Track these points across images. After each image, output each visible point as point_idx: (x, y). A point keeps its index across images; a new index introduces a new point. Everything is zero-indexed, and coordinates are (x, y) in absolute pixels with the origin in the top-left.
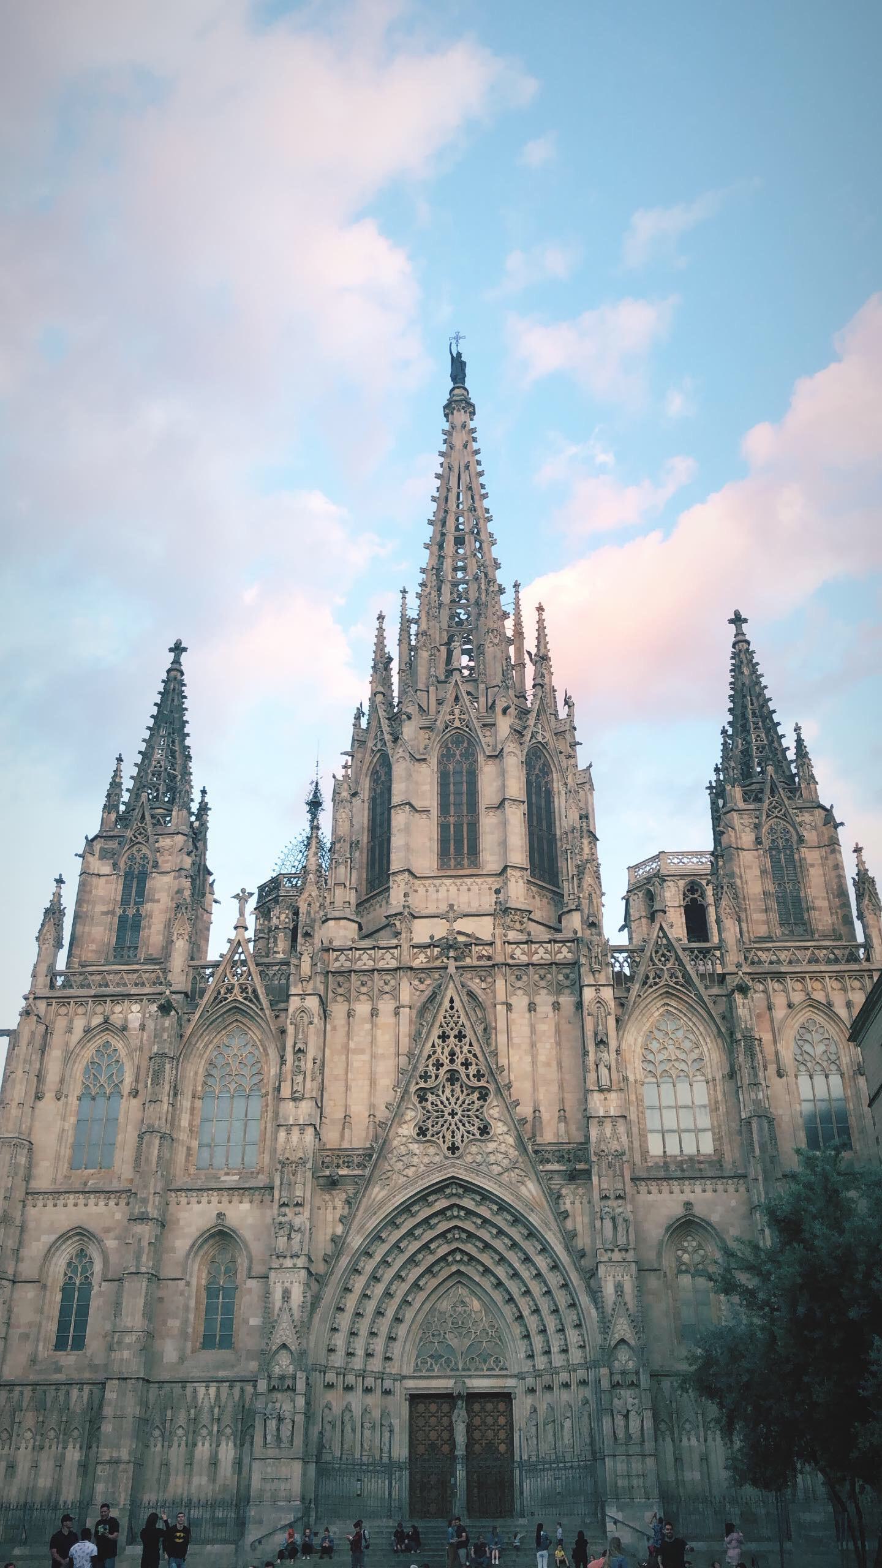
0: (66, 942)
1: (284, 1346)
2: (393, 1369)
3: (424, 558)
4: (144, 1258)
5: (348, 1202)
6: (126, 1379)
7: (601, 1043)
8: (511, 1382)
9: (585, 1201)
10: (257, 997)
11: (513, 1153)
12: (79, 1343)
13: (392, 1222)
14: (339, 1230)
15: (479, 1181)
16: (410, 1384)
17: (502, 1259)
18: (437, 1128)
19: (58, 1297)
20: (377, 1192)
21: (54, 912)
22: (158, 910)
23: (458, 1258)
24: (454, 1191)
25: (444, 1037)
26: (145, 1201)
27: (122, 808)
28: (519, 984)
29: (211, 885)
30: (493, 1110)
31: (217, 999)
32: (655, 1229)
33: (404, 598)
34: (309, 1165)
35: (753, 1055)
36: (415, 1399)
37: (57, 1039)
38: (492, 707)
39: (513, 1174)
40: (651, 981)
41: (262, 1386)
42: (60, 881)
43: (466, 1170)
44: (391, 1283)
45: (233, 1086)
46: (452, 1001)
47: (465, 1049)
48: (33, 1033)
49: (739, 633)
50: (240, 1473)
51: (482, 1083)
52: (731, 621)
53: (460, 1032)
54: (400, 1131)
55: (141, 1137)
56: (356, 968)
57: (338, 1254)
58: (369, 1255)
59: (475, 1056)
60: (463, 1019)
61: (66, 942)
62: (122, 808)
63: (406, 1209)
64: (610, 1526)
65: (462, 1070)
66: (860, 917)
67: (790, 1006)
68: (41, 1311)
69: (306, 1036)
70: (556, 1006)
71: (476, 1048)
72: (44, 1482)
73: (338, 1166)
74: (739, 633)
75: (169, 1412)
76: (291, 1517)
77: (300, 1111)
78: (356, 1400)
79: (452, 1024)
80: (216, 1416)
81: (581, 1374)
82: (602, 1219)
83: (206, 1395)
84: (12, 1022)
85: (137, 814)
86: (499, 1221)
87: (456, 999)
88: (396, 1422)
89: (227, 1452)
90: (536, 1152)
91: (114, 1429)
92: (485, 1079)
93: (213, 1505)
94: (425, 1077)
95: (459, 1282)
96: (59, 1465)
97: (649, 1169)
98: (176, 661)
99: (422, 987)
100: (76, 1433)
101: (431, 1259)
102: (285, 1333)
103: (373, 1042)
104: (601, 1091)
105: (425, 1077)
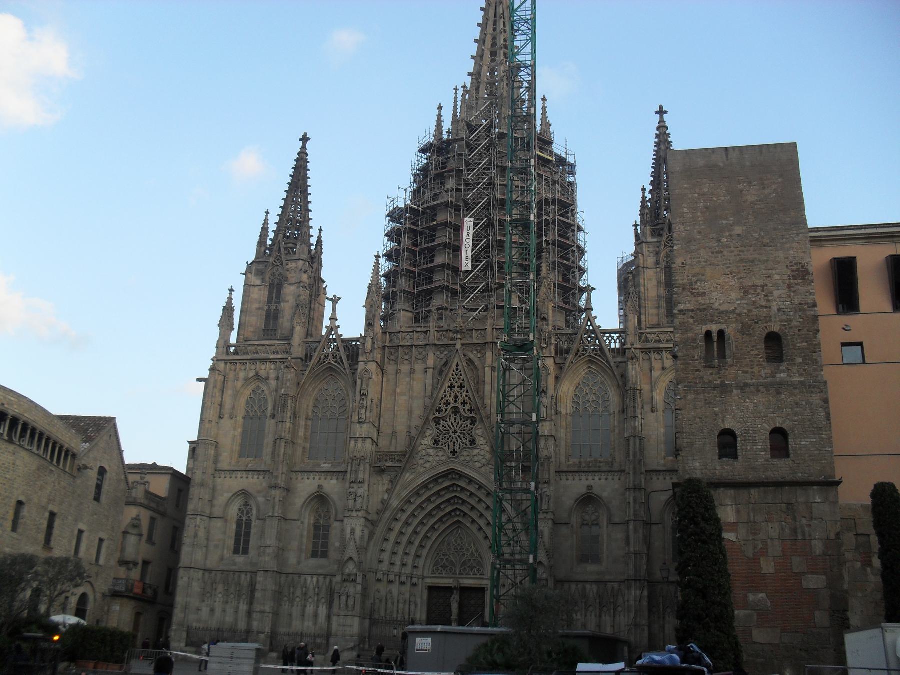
0: (236, 326)
1: (351, 559)
2: (419, 572)
3: (470, 66)
4: (277, 508)
5: (391, 482)
10: (342, 361)
11: (489, 456)
12: (246, 551)
13: (418, 494)
15: (467, 471)
16: (429, 581)
17: (482, 515)
19: (234, 526)
20: (408, 477)
21: (228, 310)
22: (287, 307)
25: (451, 387)
26: (277, 477)
27: (269, 243)
29: (325, 289)
30: (478, 432)
31: (320, 362)
32: (569, 501)
33: (456, 94)
34: (367, 461)
35: (635, 400)
36: (432, 589)
37: (230, 384)
41: (338, 579)
42: (231, 290)
44: (417, 526)
45: (328, 414)
46: (457, 365)
47: (464, 395)
48: (216, 381)
49: (662, 121)
52: (657, 113)
54: (423, 442)
55: (275, 442)
56: (401, 344)
57: (384, 510)
58: (403, 511)
59: (470, 398)
60: (464, 376)
61: (236, 326)
62: (269, 243)
63: (425, 486)
65: (461, 407)
67: (663, 369)
68: (225, 533)
69: (368, 386)
71: (470, 394)
72: (229, 619)
73: (386, 461)
74: (662, 121)
75: (292, 589)
76: (352, 645)
78: (395, 589)
83: (311, 582)
84: (206, 375)
85: (275, 248)
86: (479, 494)
88: (419, 601)
89: (323, 611)
93: (315, 637)
94: (439, 411)
96: (237, 612)
97: (569, 466)
98: (304, 148)
99: (442, 356)
100: (244, 597)
101: (442, 514)
102: (351, 552)
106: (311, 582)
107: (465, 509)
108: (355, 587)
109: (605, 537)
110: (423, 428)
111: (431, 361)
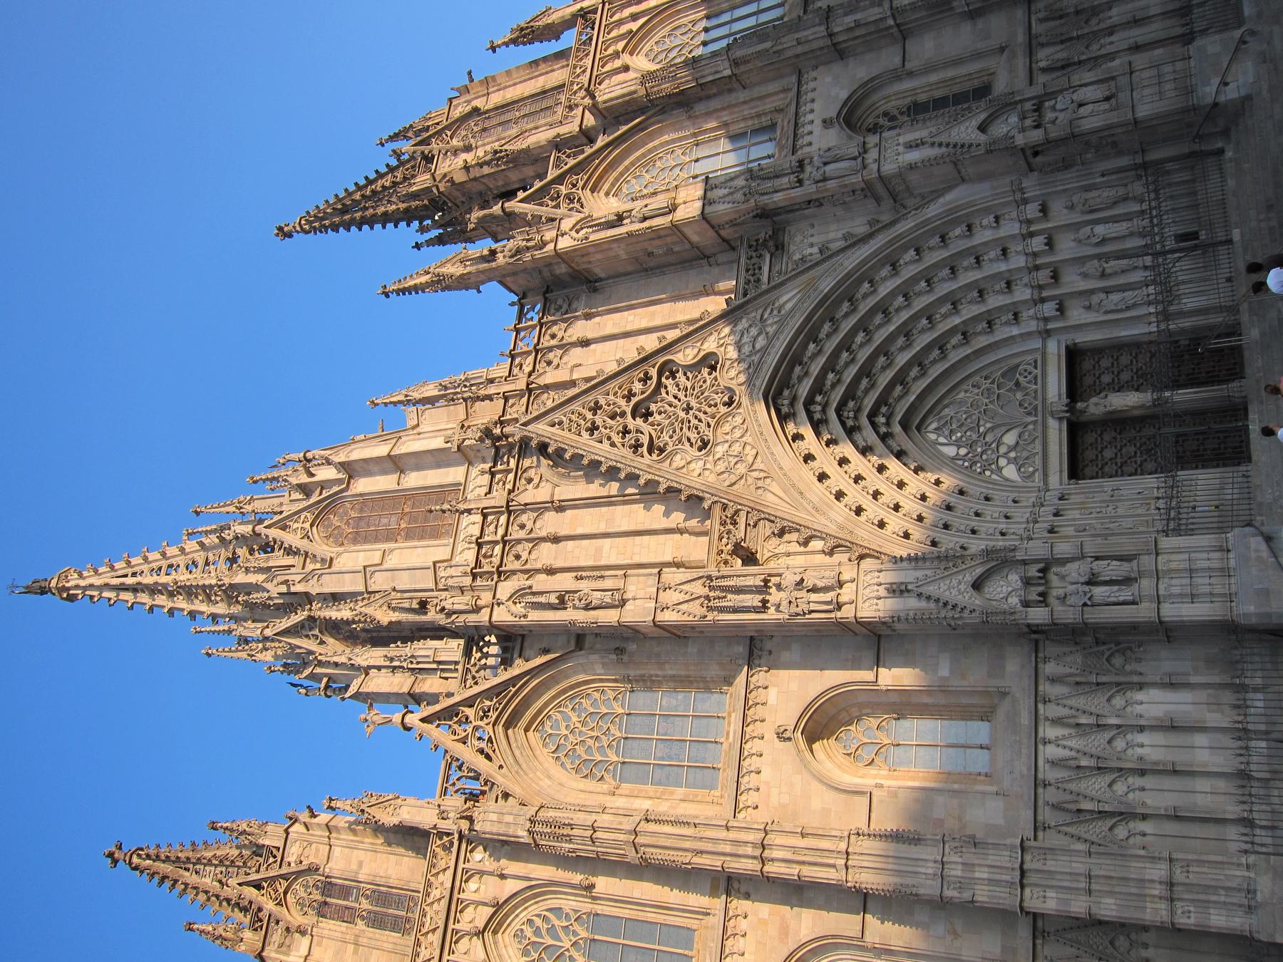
1: (977, 585)
5: (782, 533)
6: (1023, 873)
7: (620, 219)
8: (1055, 349)
11: (744, 323)
14: (816, 545)
16: (1054, 480)
17: (883, 350)
18: (702, 426)
23: (883, 420)
24: (786, 402)
25: (593, 428)
28: (555, 362)
36: (1075, 471)
38: (305, 490)
39: (769, 322)
43: (757, 378)
46: (553, 426)
51: (653, 372)
60: (576, 406)
64: (1231, 93)
65: (634, 400)
66: (553, 32)
67: (626, 68)
76: (1257, 543)
77: (641, 594)
80: (1092, 720)
81: (1032, 210)
82: (825, 179)
83: (1059, 743)
86: (830, 347)
90: (745, 295)
91: (1111, 893)
95: (919, 428)
99: (536, 481)
104: (673, 208)
105: (636, 447)
106: (1059, 743)
107: (869, 403)
108: (1063, 562)
109: (934, 78)
111: (541, 494)
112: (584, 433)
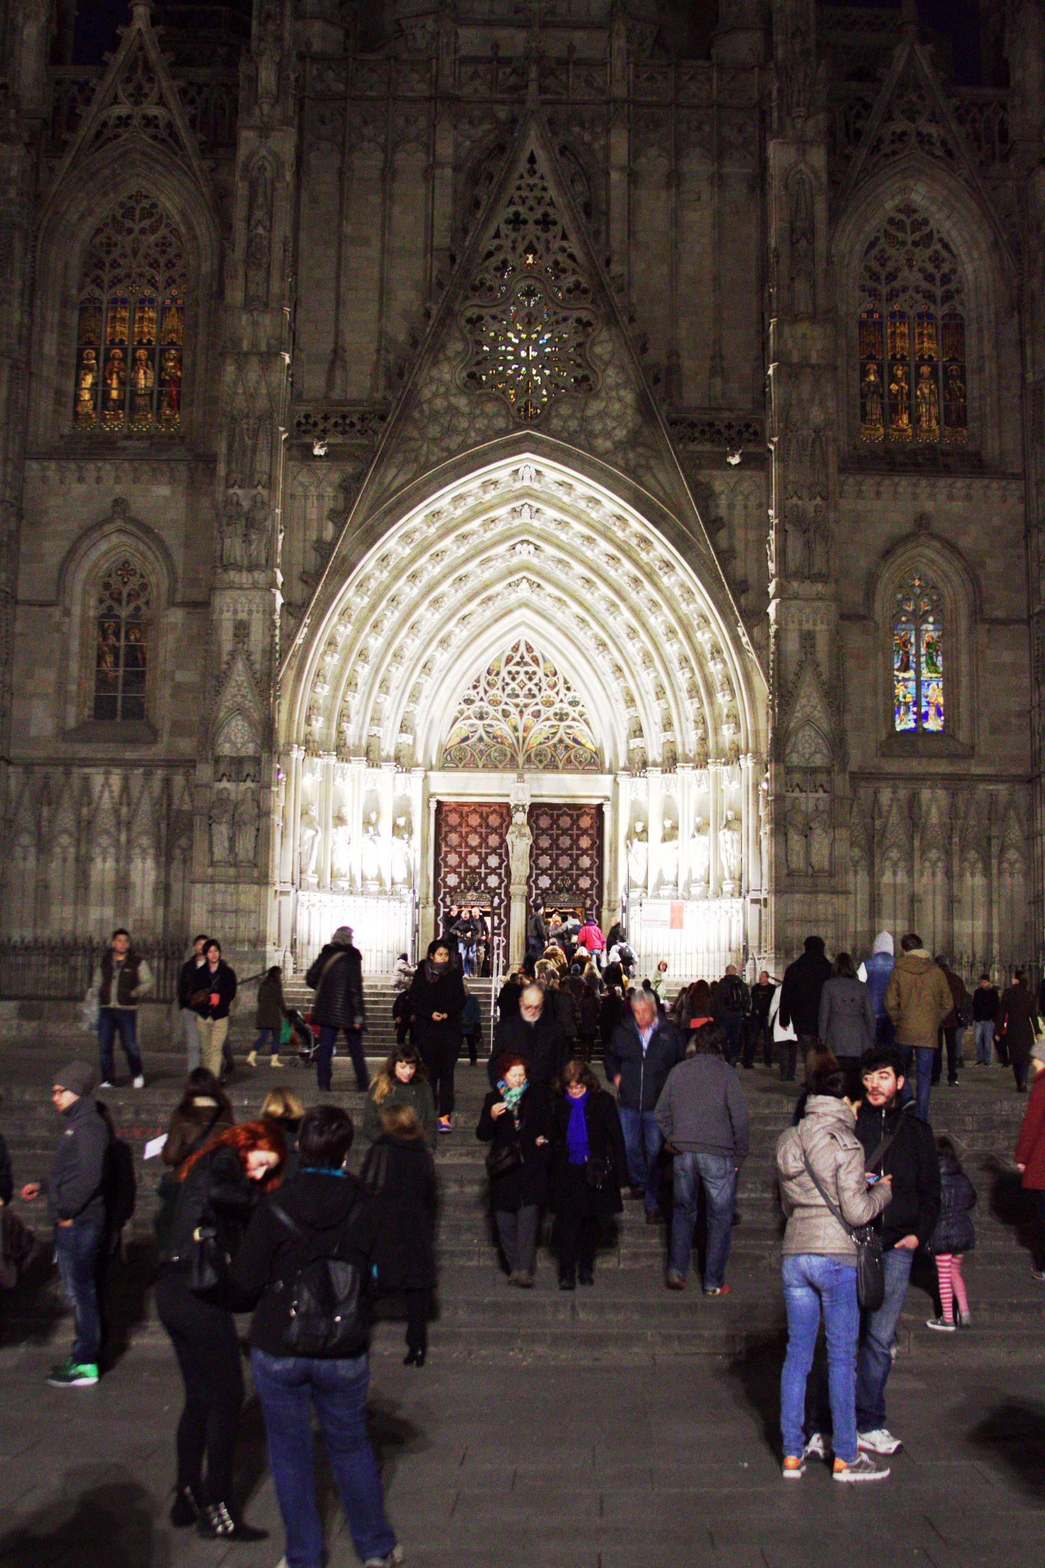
9: (753, 502)
10: (174, 135)
40: (887, 149)
47: (556, 244)
50: (167, 904)
53: (546, 215)
59: (571, 257)
60: (553, 193)
70: (719, 181)
75: (45, 811)
79: (532, 202)
83: (106, 786)
87: (541, 155)
89: (144, 872)
92: (590, 297)
103: (386, 227)
110: (436, 335)
111: (445, 149)
112: (512, 209)
